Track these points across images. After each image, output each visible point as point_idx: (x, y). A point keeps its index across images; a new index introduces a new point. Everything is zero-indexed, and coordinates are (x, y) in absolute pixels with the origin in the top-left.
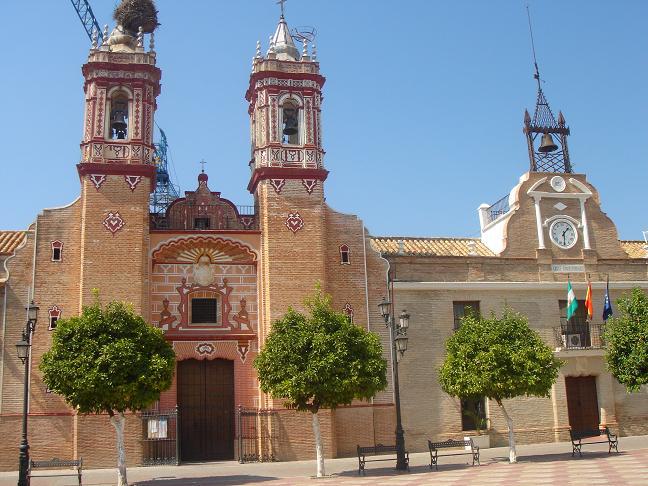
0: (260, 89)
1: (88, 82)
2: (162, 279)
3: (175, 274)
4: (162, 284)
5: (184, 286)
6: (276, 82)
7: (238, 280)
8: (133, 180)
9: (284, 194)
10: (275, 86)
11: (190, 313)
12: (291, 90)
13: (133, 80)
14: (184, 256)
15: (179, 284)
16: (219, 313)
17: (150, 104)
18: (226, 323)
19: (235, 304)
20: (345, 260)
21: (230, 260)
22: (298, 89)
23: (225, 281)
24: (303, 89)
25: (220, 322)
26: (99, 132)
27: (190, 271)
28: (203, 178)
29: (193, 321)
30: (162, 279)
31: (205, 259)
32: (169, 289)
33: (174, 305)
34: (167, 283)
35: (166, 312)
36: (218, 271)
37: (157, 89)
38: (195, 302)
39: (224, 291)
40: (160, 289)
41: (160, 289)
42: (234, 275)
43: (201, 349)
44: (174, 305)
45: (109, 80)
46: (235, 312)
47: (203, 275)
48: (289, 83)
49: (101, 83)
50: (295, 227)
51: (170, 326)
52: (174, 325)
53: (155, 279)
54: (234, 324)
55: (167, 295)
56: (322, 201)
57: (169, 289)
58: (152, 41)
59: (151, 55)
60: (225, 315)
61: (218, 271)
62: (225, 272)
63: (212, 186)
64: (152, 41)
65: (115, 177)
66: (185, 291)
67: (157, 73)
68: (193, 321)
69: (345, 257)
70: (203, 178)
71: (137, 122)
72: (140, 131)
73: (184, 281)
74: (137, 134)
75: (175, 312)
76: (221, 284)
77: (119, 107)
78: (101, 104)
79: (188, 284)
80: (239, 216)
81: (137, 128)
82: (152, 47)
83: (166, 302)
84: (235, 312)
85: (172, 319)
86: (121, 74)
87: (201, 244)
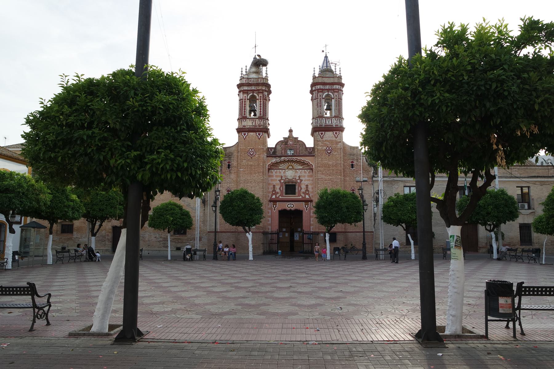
0: (315, 90)
1: (240, 92)
2: (272, 176)
3: (278, 174)
4: (272, 178)
5: (282, 179)
6: (322, 87)
7: (304, 176)
8: (259, 134)
9: (324, 139)
10: (321, 89)
11: (284, 191)
12: (328, 90)
13: (258, 90)
14: (282, 166)
15: (280, 178)
16: (297, 191)
17: (266, 100)
18: (300, 195)
19: (303, 187)
20: (352, 167)
21: (301, 167)
22: (331, 90)
23: (299, 177)
24: (334, 90)
25: (297, 195)
26: (245, 114)
27: (284, 173)
28: (291, 131)
29: (286, 194)
30: (272, 176)
31: (290, 167)
32: (276, 180)
33: (278, 187)
34: (275, 178)
35: (274, 190)
36: (296, 172)
37: (270, 92)
38: (286, 185)
39: (299, 181)
40: (272, 180)
41: (272, 180)
42: (303, 174)
43: (289, 206)
44: (278, 187)
45: (248, 90)
46: (303, 190)
47: (290, 174)
48: (327, 87)
49: (244, 92)
50: (329, 153)
51: (276, 196)
52: (278, 196)
53: (269, 176)
54: (303, 195)
55: (274, 183)
56: (341, 141)
57: (276, 180)
58: (266, 71)
59: (266, 79)
60: (299, 191)
61: (296, 172)
62: (299, 173)
63: (295, 135)
64: (266, 71)
65: (252, 134)
66: (282, 181)
67: (268, 86)
68: (286, 194)
69: (352, 166)
70: (291, 131)
71: (260, 109)
72: (262, 113)
73: (282, 177)
74: (260, 114)
75: (278, 190)
76: (298, 178)
77: (253, 100)
78: (245, 102)
79: (283, 178)
80: (307, 148)
81: (260, 112)
82: (266, 74)
83: (274, 186)
84: (303, 190)
85: (276, 193)
86: (253, 88)
87: (288, 161)
